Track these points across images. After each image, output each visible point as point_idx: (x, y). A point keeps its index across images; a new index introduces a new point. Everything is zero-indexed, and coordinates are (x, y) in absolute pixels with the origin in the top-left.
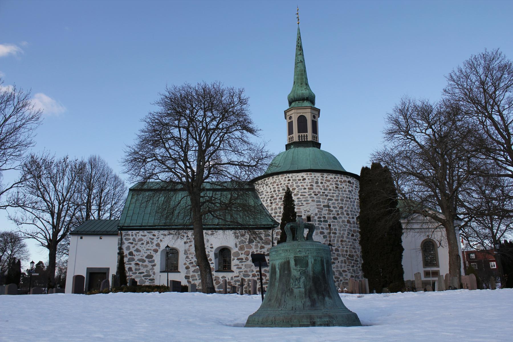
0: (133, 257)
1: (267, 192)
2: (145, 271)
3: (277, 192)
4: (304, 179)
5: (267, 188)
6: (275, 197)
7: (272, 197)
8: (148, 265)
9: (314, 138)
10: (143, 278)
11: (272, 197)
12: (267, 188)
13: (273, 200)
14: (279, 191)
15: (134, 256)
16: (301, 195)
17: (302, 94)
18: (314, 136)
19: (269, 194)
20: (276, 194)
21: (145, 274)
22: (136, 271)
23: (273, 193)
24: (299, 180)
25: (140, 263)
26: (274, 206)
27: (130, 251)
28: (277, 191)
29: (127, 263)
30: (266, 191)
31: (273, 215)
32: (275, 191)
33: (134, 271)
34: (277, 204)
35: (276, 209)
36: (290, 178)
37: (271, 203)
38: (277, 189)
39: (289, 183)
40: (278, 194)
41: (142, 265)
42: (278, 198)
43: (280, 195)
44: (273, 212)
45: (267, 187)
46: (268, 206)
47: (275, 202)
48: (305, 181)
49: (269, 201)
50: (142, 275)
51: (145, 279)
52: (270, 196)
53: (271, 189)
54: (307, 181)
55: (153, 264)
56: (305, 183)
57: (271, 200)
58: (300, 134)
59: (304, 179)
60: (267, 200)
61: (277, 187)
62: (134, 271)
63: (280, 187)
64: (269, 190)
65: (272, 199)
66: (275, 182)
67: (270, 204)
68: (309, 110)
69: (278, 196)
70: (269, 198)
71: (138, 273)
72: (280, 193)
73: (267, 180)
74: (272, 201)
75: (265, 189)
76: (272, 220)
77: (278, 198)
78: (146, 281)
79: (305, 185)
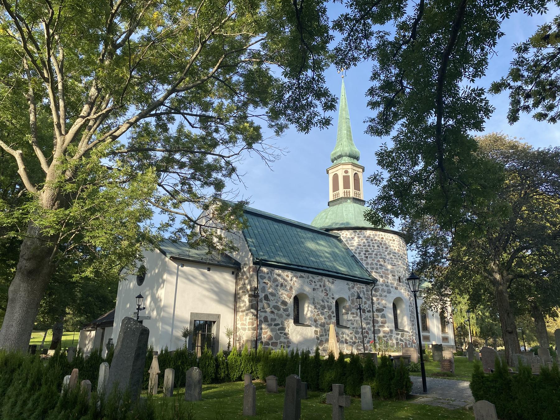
0: (269, 302)
2: (280, 323)
3: (371, 247)
4: (394, 240)
6: (371, 252)
7: (367, 251)
8: (283, 314)
10: (278, 332)
11: (367, 251)
13: (369, 254)
14: (374, 246)
15: (270, 301)
16: (393, 255)
17: (356, 152)
20: (371, 249)
21: (281, 326)
22: (272, 322)
23: (367, 247)
24: (391, 240)
25: (276, 311)
26: (369, 261)
27: (265, 294)
28: (371, 246)
29: (262, 310)
31: (369, 270)
32: (369, 246)
33: (270, 322)
34: (373, 260)
35: (372, 264)
36: (383, 236)
37: (367, 257)
38: (371, 245)
39: (382, 241)
40: (373, 250)
41: (277, 314)
42: (374, 253)
43: (375, 251)
44: (369, 266)
46: (362, 259)
47: (371, 257)
48: (395, 242)
49: (362, 254)
50: (277, 327)
51: (281, 333)
52: (364, 250)
54: (395, 242)
55: (287, 313)
56: (394, 244)
57: (365, 254)
59: (394, 240)
60: (360, 253)
61: (371, 242)
62: (270, 322)
65: (367, 253)
67: (364, 258)
68: (350, 166)
69: (373, 251)
70: (362, 251)
71: (273, 324)
72: (375, 249)
74: (367, 255)
76: (369, 275)
77: (374, 253)
78: (281, 336)
79: (395, 245)
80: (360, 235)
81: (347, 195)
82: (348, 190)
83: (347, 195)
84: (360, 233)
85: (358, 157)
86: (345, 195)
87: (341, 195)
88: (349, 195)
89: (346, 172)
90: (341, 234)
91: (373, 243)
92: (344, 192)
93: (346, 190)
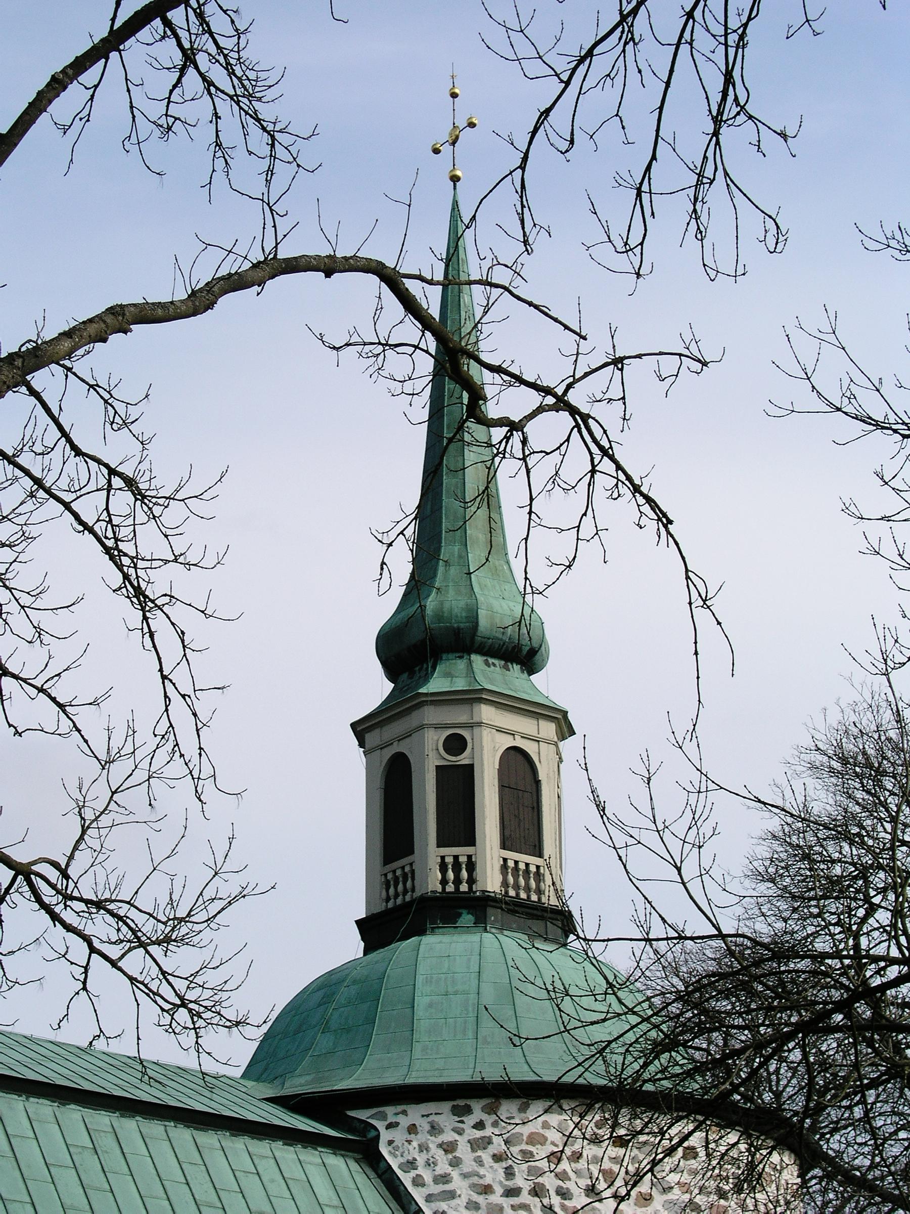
1: (487, 1190)
5: (479, 1162)
9: (511, 879)
12: (479, 1162)
18: (511, 864)
19: (496, 1198)
30: (475, 1180)
38: (550, 1182)
45: (486, 1156)
53: (509, 1173)
58: (512, 855)
63: (572, 1175)
64: (493, 1174)
66: (536, 1139)
73: (478, 1114)
75: (468, 1165)
80: (488, 1131)
81: (457, 881)
82: (463, 852)
83: (457, 881)
84: (489, 1119)
85: (533, 652)
86: (444, 882)
87: (432, 881)
88: (471, 881)
89: (456, 744)
90: (380, 1125)
91: (562, 1176)
92: (443, 867)
93: (449, 852)
